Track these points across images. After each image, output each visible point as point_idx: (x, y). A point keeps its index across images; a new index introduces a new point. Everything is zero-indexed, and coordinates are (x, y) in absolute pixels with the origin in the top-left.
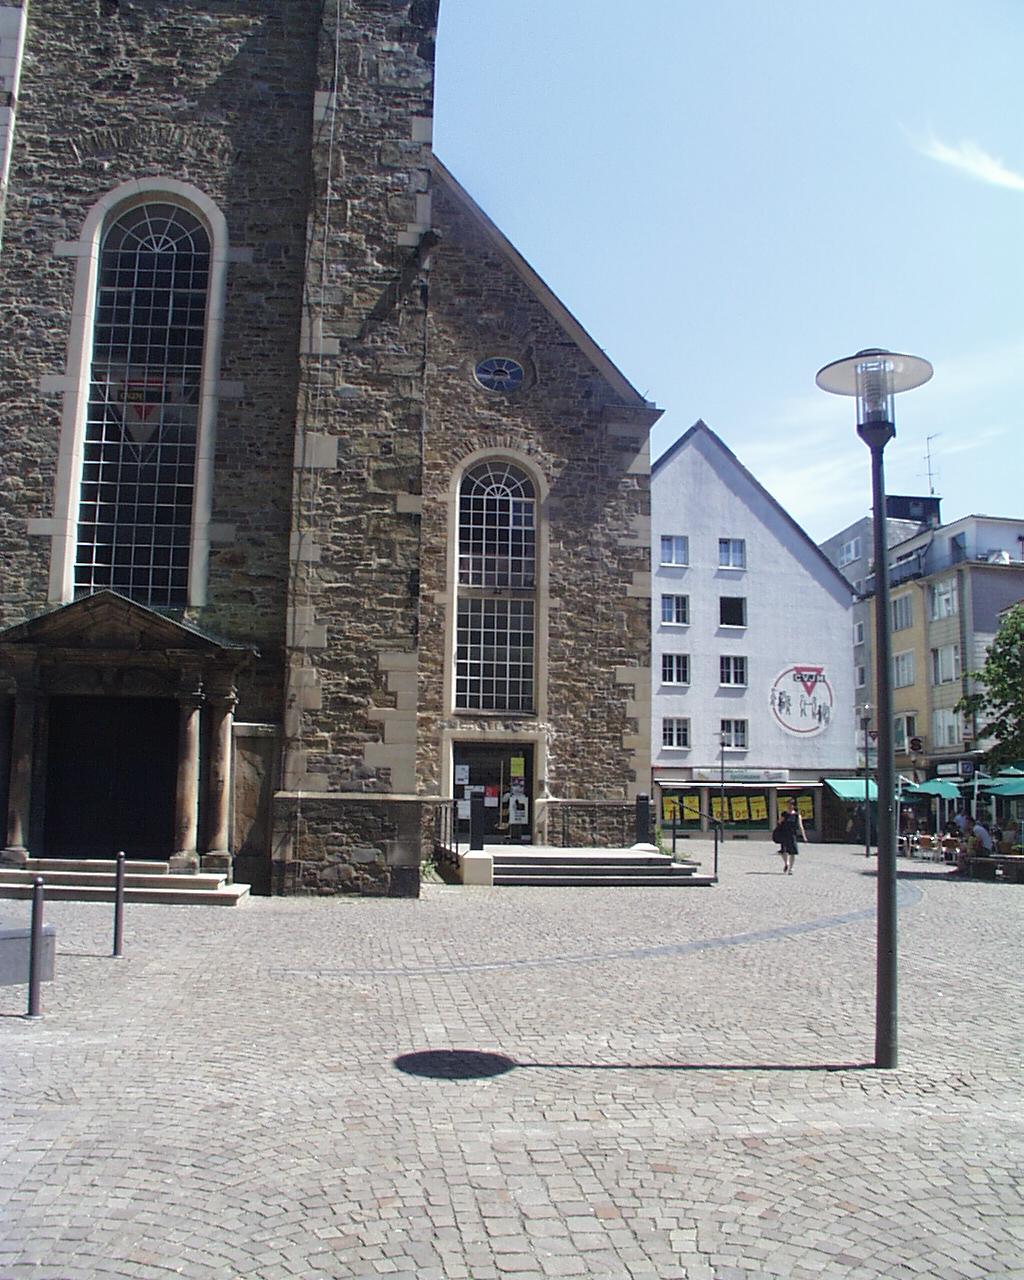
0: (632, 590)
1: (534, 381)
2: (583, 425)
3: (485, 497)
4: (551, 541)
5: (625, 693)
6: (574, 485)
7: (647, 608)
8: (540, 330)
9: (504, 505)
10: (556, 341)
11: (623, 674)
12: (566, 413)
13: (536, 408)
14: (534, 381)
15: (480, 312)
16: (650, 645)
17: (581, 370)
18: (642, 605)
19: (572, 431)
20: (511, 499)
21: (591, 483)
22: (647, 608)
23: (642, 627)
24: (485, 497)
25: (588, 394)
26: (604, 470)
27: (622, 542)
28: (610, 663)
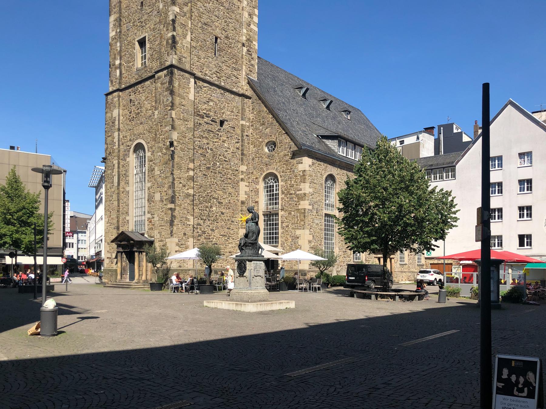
0: (300, 207)
1: (278, 147)
2: (289, 158)
3: (269, 185)
4: (281, 195)
5: (298, 238)
6: (287, 177)
7: (304, 212)
8: (279, 131)
9: (273, 186)
10: (283, 133)
11: (298, 232)
12: (284, 156)
13: (278, 156)
14: (278, 147)
15: (265, 130)
16: (304, 223)
17: (289, 141)
18: (303, 211)
19: (286, 161)
20: (275, 184)
21: (291, 176)
22: (304, 212)
23: (302, 217)
24: (269, 185)
25: (290, 148)
26: (294, 171)
27: (298, 193)
28: (295, 229)
